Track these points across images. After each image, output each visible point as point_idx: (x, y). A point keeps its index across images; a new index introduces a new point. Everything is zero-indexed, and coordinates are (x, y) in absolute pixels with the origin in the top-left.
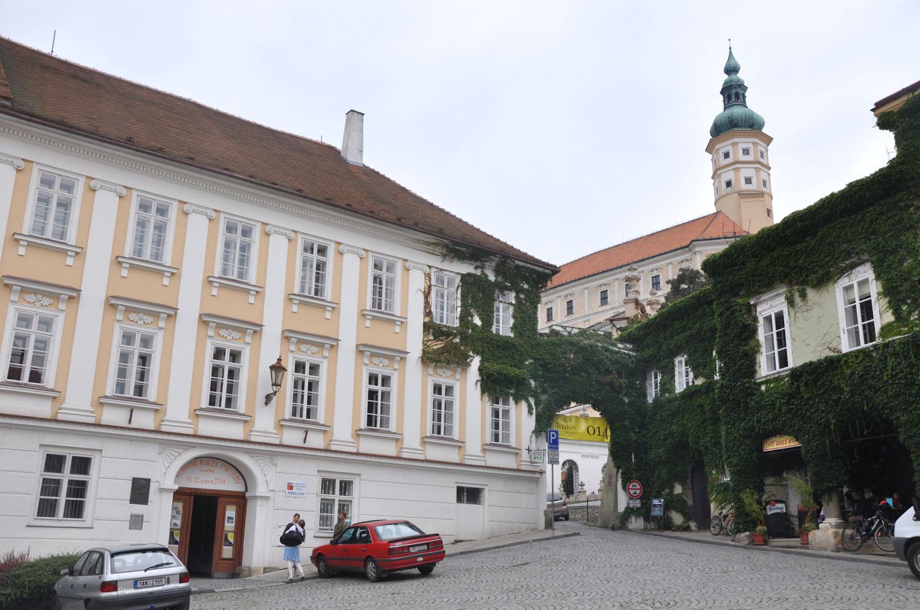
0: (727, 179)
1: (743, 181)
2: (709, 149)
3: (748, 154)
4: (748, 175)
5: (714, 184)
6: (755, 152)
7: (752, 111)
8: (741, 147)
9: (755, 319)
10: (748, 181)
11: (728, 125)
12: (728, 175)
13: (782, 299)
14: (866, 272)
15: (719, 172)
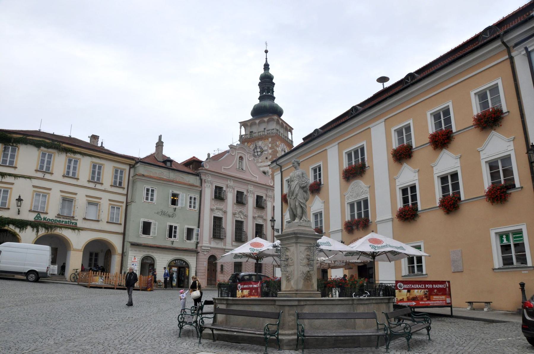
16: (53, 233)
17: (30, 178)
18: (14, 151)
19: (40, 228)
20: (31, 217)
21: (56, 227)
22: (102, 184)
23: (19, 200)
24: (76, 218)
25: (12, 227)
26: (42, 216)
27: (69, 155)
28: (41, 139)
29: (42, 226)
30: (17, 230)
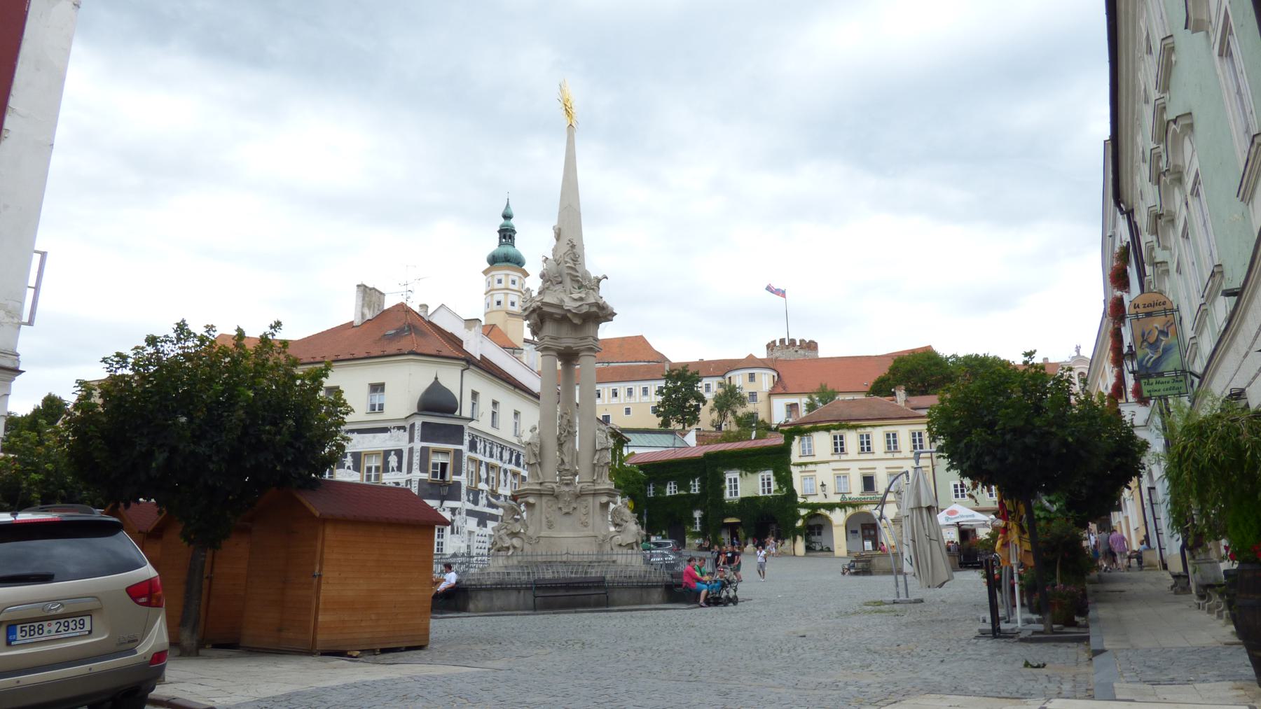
0: (499, 299)
1: (509, 304)
2: (486, 272)
3: (514, 284)
4: (513, 300)
5: (485, 299)
6: (519, 284)
7: (521, 255)
8: (511, 278)
9: (725, 478)
10: (513, 304)
11: (504, 259)
12: (499, 296)
13: (738, 474)
14: (769, 473)
15: (491, 293)
16: (860, 511)
17: (827, 462)
18: (809, 440)
19: (847, 508)
20: (837, 499)
21: (862, 504)
22: (900, 452)
23: (823, 485)
24: (879, 493)
25: (823, 511)
26: (847, 496)
27: (859, 431)
28: (829, 424)
29: (849, 506)
30: (828, 513)
